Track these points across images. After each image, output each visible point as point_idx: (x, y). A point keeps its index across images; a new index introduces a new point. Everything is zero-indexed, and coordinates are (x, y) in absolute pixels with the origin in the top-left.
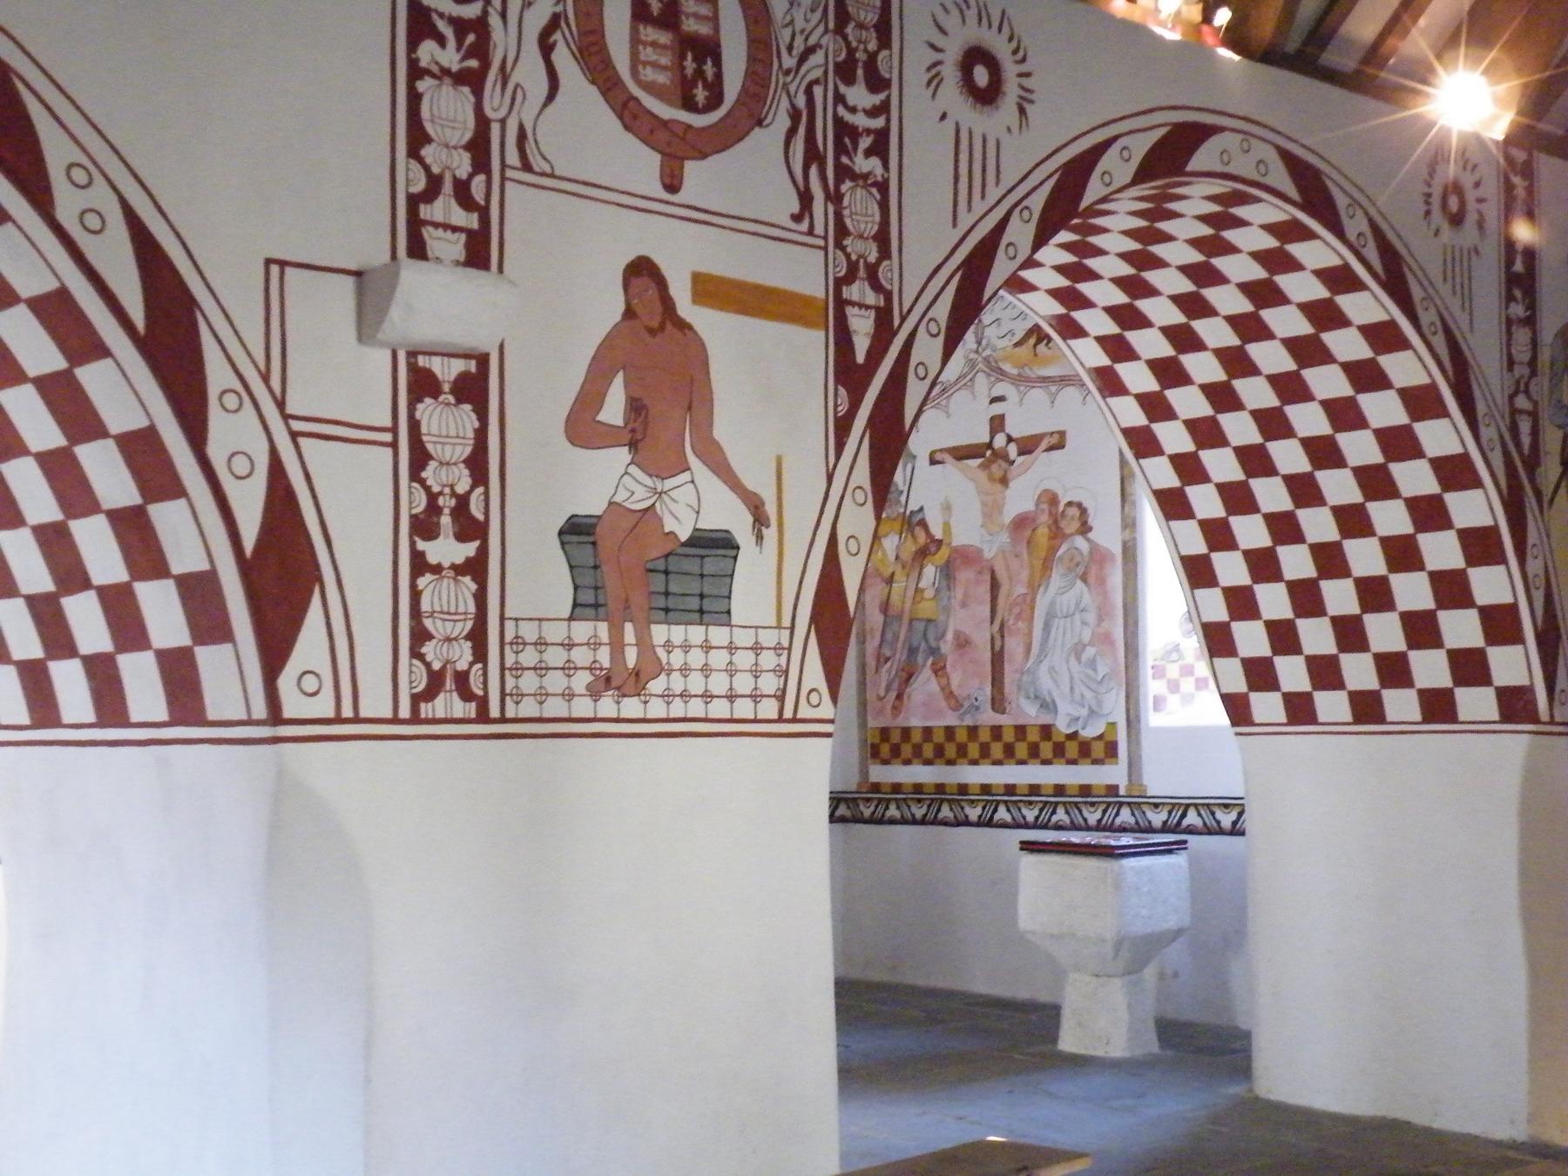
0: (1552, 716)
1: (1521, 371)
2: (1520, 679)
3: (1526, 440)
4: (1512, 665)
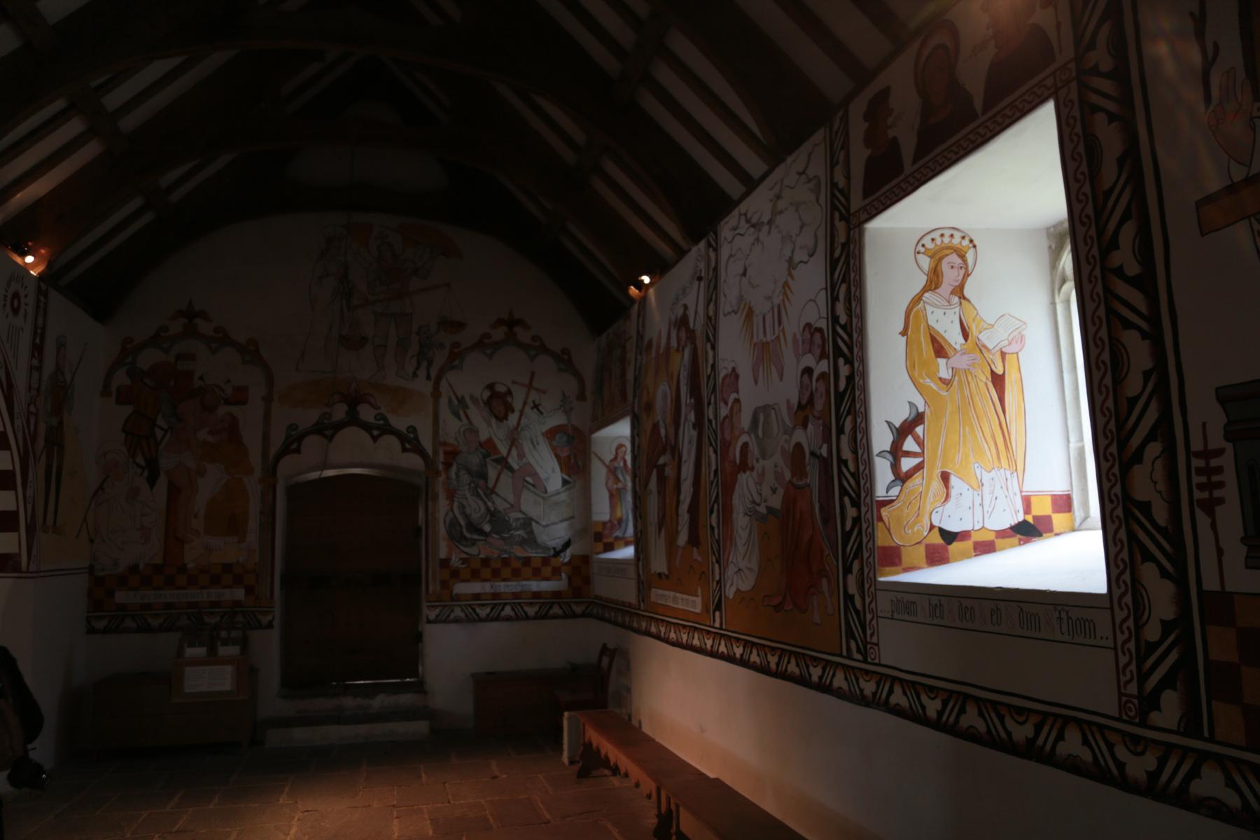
3: (32, 428)
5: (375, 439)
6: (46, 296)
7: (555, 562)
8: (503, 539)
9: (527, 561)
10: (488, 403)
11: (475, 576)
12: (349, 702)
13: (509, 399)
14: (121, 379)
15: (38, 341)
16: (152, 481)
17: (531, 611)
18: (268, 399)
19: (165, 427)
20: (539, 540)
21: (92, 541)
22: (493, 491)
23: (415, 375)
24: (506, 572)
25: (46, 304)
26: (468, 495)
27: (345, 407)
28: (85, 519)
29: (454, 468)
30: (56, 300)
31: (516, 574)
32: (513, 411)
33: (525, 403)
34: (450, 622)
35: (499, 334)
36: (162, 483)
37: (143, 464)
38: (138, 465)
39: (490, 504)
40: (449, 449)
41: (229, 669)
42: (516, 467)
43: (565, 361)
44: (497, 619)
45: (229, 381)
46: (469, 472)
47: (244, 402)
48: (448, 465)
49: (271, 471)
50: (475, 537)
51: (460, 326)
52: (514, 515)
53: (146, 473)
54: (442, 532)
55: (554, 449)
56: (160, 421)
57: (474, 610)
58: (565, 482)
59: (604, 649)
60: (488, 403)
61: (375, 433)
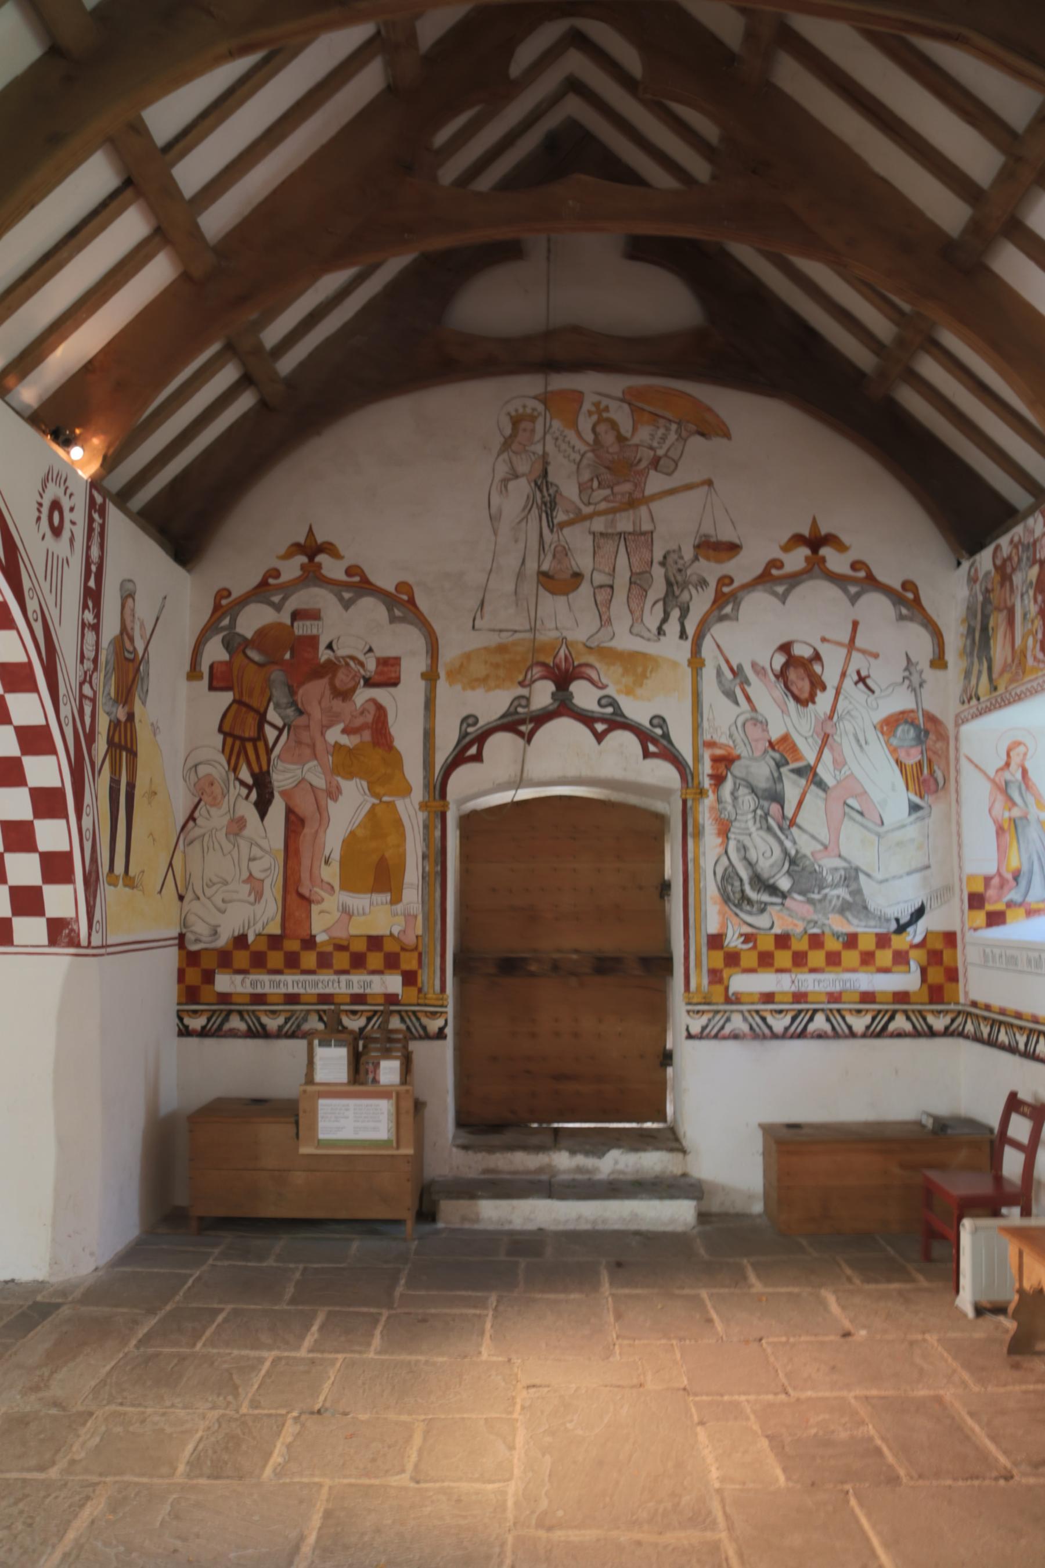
0: (89, 942)
1: (88, 665)
2: (68, 913)
4: (61, 900)
5: (599, 737)
6: (102, 513)
7: (899, 942)
8: (811, 901)
9: (851, 941)
10: (782, 675)
11: (765, 961)
12: (564, 1162)
13: (817, 668)
14: (215, 652)
15: (92, 583)
16: (262, 807)
17: (859, 1024)
18: (430, 677)
19: (280, 723)
20: (871, 906)
21: (181, 898)
22: (793, 823)
23: (660, 631)
24: (817, 958)
25: (102, 526)
26: (753, 829)
27: (549, 687)
28: (171, 865)
29: (728, 785)
30: (116, 520)
31: (833, 960)
32: (824, 688)
33: (843, 675)
34: (725, 1038)
35: (796, 559)
36: (277, 809)
37: (250, 781)
38: (243, 783)
39: (788, 844)
40: (719, 752)
41: (384, 1107)
42: (830, 781)
43: (908, 601)
44: (802, 1035)
45: (370, 650)
46: (753, 791)
47: (395, 683)
48: (718, 780)
49: (438, 789)
50: (765, 898)
51: (733, 548)
52: (828, 863)
53: (254, 795)
54: (711, 889)
55: (893, 751)
56: (272, 715)
57: (764, 1019)
58: (914, 808)
59: (1013, 1103)
60: (782, 675)
61: (600, 727)
